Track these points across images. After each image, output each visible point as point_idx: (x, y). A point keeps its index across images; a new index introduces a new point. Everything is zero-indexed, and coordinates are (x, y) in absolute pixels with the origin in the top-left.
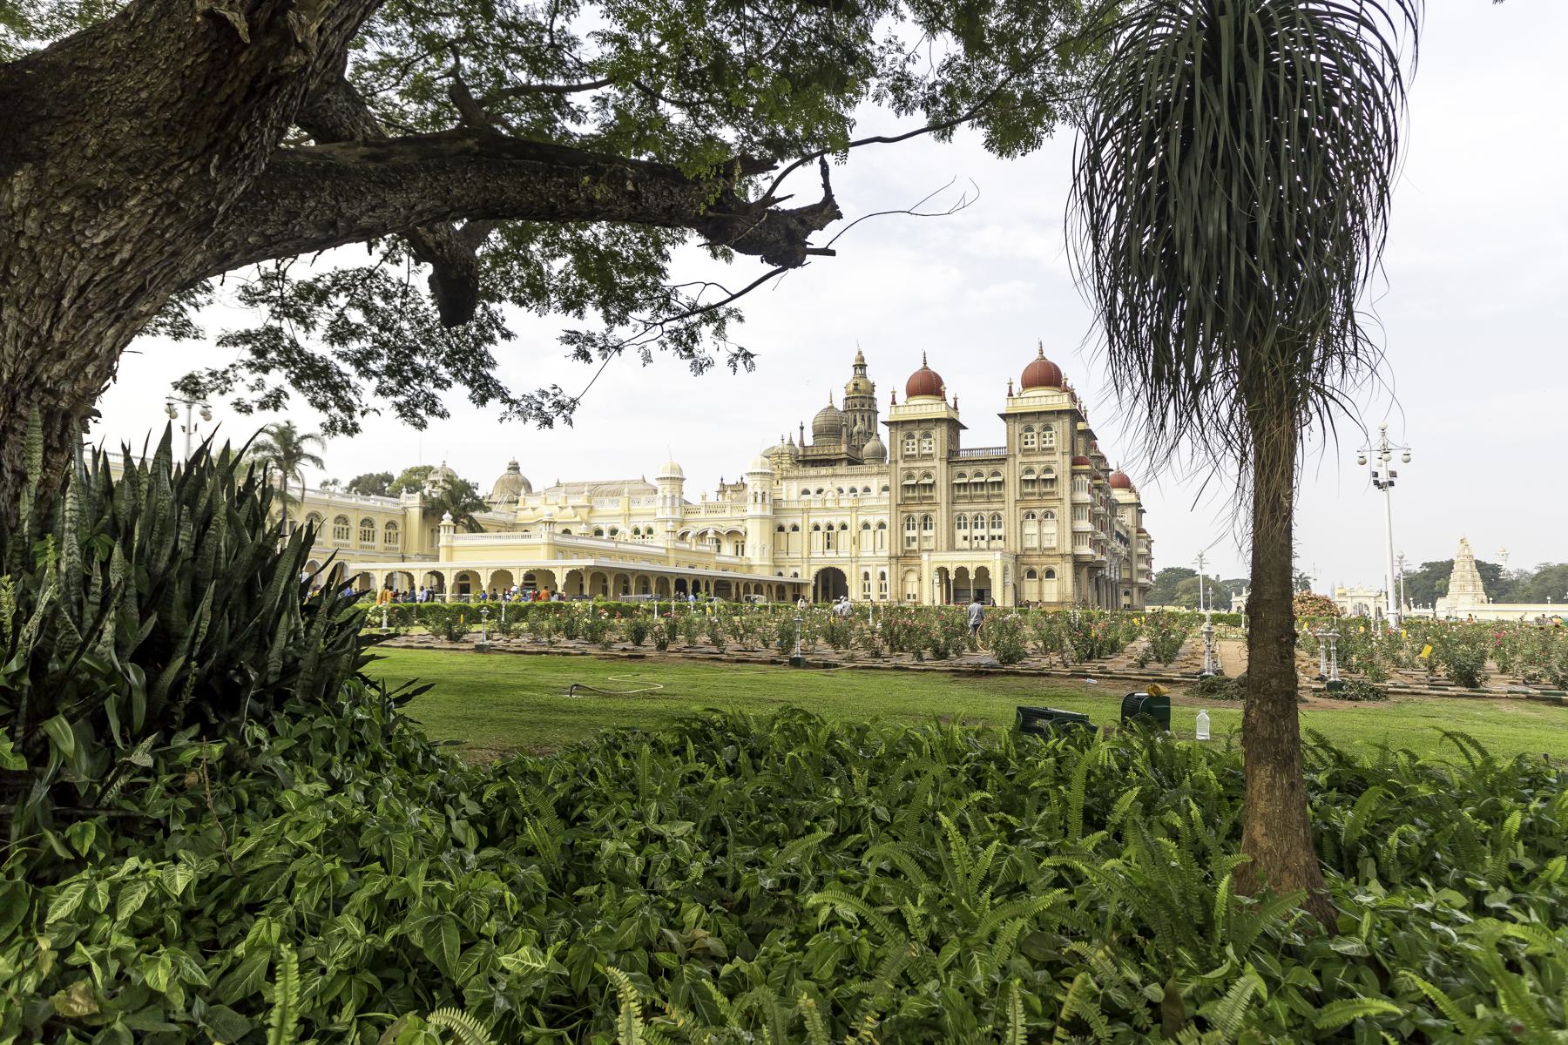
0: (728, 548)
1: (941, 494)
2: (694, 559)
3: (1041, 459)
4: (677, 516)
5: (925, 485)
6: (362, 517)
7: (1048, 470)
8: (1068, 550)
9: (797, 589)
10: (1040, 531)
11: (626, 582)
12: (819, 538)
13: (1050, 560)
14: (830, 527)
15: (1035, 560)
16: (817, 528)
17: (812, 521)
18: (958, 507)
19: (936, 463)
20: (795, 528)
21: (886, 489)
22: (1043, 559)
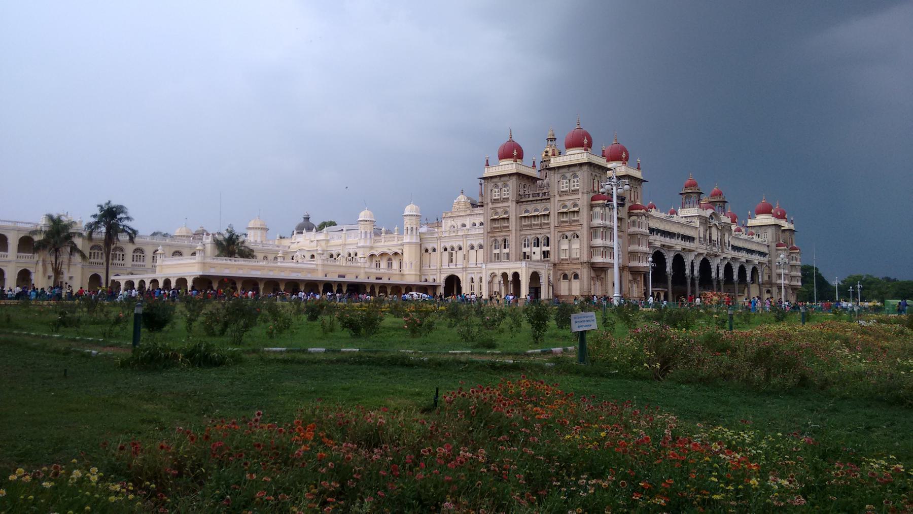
1: (513, 224)
2: (342, 271)
3: (570, 197)
7: (575, 205)
8: (585, 260)
9: (434, 288)
10: (570, 247)
11: (234, 283)
12: (446, 254)
13: (575, 267)
14: (453, 249)
15: (566, 267)
16: (446, 250)
17: (443, 245)
18: (523, 233)
19: (509, 203)
20: (434, 250)
21: (481, 224)
22: (571, 267)
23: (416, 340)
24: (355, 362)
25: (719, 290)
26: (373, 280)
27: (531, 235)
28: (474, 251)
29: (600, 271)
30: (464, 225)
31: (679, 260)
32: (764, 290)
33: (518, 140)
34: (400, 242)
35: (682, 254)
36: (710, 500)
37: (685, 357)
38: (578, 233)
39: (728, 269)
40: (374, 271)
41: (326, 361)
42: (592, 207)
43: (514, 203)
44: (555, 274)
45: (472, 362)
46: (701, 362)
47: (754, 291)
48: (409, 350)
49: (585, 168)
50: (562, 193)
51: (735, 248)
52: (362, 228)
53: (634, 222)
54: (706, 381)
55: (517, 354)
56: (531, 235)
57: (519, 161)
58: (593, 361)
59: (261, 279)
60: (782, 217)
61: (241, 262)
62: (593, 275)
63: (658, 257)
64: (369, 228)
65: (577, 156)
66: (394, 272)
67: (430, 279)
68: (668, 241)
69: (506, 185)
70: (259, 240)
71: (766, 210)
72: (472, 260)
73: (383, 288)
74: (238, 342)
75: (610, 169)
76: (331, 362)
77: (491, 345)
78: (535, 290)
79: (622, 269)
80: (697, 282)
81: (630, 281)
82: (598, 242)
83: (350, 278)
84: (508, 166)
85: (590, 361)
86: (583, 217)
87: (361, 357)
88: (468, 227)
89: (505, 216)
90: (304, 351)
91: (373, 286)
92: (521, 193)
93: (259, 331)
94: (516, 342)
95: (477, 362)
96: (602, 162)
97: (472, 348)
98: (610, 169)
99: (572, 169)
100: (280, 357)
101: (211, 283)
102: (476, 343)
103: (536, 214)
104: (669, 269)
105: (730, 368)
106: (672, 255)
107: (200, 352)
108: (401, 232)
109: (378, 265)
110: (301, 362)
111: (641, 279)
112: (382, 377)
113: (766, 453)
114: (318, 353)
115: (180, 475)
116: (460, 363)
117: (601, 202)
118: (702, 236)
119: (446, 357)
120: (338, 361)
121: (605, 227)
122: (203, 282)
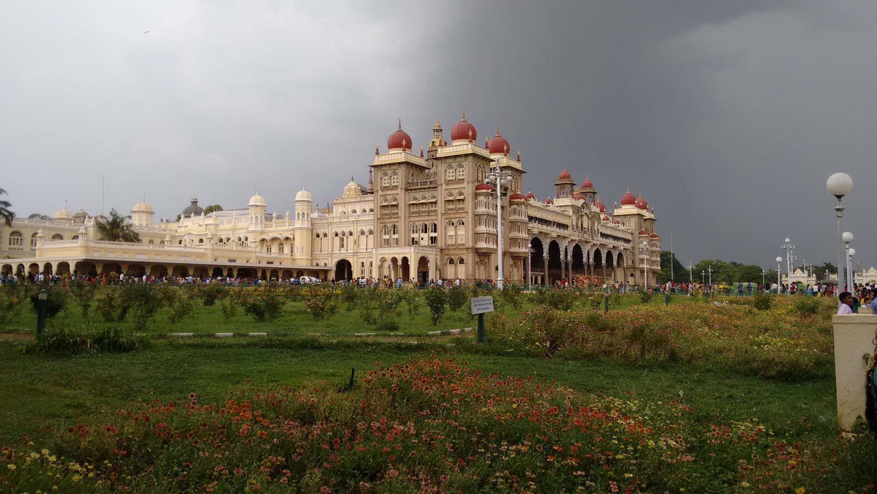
0: (287, 249)
1: (402, 211)
2: (233, 256)
3: (456, 186)
4: (259, 229)
5: (393, 205)
6: (54, 233)
7: (461, 194)
8: (470, 245)
9: (326, 272)
10: (456, 233)
12: (337, 239)
13: (461, 252)
14: (344, 234)
15: (452, 252)
16: (337, 235)
17: (334, 230)
18: (412, 219)
19: (399, 191)
20: (325, 235)
21: (372, 210)
22: (457, 252)
23: (319, 323)
24: (266, 346)
25: (590, 273)
26: (264, 264)
27: (419, 221)
28: (364, 237)
29: (483, 256)
30: (354, 211)
31: (554, 246)
32: (629, 274)
33: (407, 130)
34: (291, 227)
35: (557, 241)
36: (614, 459)
37: (571, 336)
38: (464, 220)
39: (598, 254)
40: (265, 255)
41: (236, 345)
42: (476, 195)
43: (403, 191)
44: (442, 259)
45: (379, 344)
46: (585, 340)
47: (620, 275)
48: (316, 332)
49: (470, 159)
50: (448, 182)
51: (604, 235)
52: (252, 212)
53: (515, 209)
54: (590, 357)
55: (419, 336)
56: (419, 221)
57: (408, 151)
58: (490, 341)
59: (148, 264)
60: (644, 207)
61: (126, 246)
62: (477, 260)
63: (536, 243)
64: (260, 213)
65: (462, 147)
66: (286, 256)
67: (322, 264)
68: (545, 228)
69: (395, 173)
70: (144, 224)
71: (630, 201)
72: (363, 246)
73: (275, 272)
74: (141, 327)
75: (492, 161)
76: (243, 346)
77: (393, 328)
78: (423, 274)
79: (504, 254)
80: (570, 267)
81: (511, 266)
82: (482, 228)
83: (241, 263)
84: (397, 155)
85: (487, 342)
86: (469, 205)
87: (271, 341)
88: (358, 213)
89: (394, 203)
90: (212, 335)
91: (264, 271)
92: (410, 181)
93: (162, 315)
94: (415, 324)
95: (384, 344)
96: (485, 153)
97: (375, 330)
98: (492, 161)
99: (458, 159)
100: (189, 342)
101: (94, 267)
102: (379, 326)
103: (424, 201)
104: (545, 254)
105: (611, 345)
106: (548, 241)
107: (109, 337)
108: (292, 217)
109: (269, 250)
110: (212, 347)
111: (520, 264)
112: (294, 359)
113: (651, 419)
114: (227, 337)
115: (128, 455)
116: (367, 344)
117: (485, 191)
118: (574, 224)
119: (353, 340)
120: (248, 345)
121: (488, 215)
122: (87, 267)
